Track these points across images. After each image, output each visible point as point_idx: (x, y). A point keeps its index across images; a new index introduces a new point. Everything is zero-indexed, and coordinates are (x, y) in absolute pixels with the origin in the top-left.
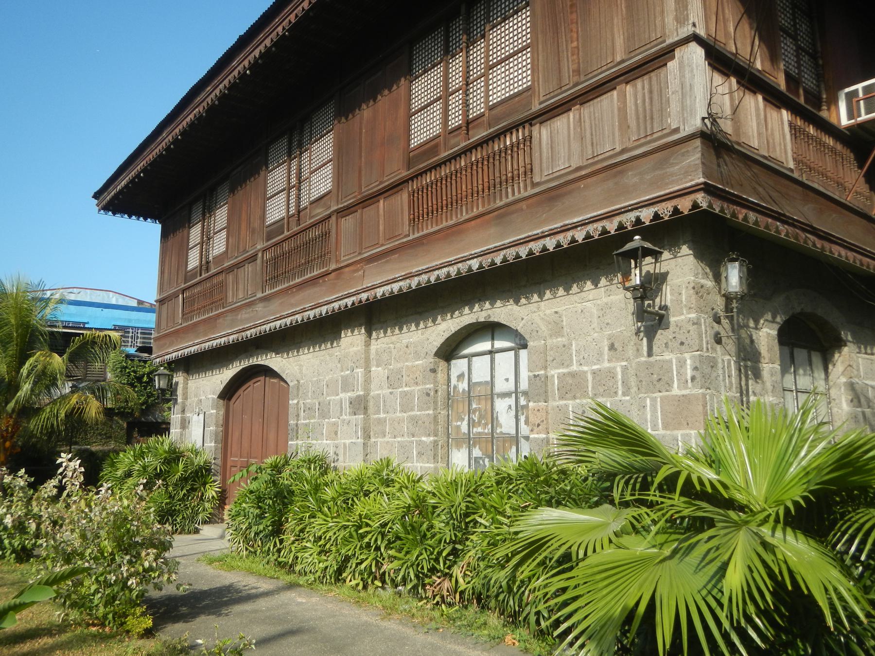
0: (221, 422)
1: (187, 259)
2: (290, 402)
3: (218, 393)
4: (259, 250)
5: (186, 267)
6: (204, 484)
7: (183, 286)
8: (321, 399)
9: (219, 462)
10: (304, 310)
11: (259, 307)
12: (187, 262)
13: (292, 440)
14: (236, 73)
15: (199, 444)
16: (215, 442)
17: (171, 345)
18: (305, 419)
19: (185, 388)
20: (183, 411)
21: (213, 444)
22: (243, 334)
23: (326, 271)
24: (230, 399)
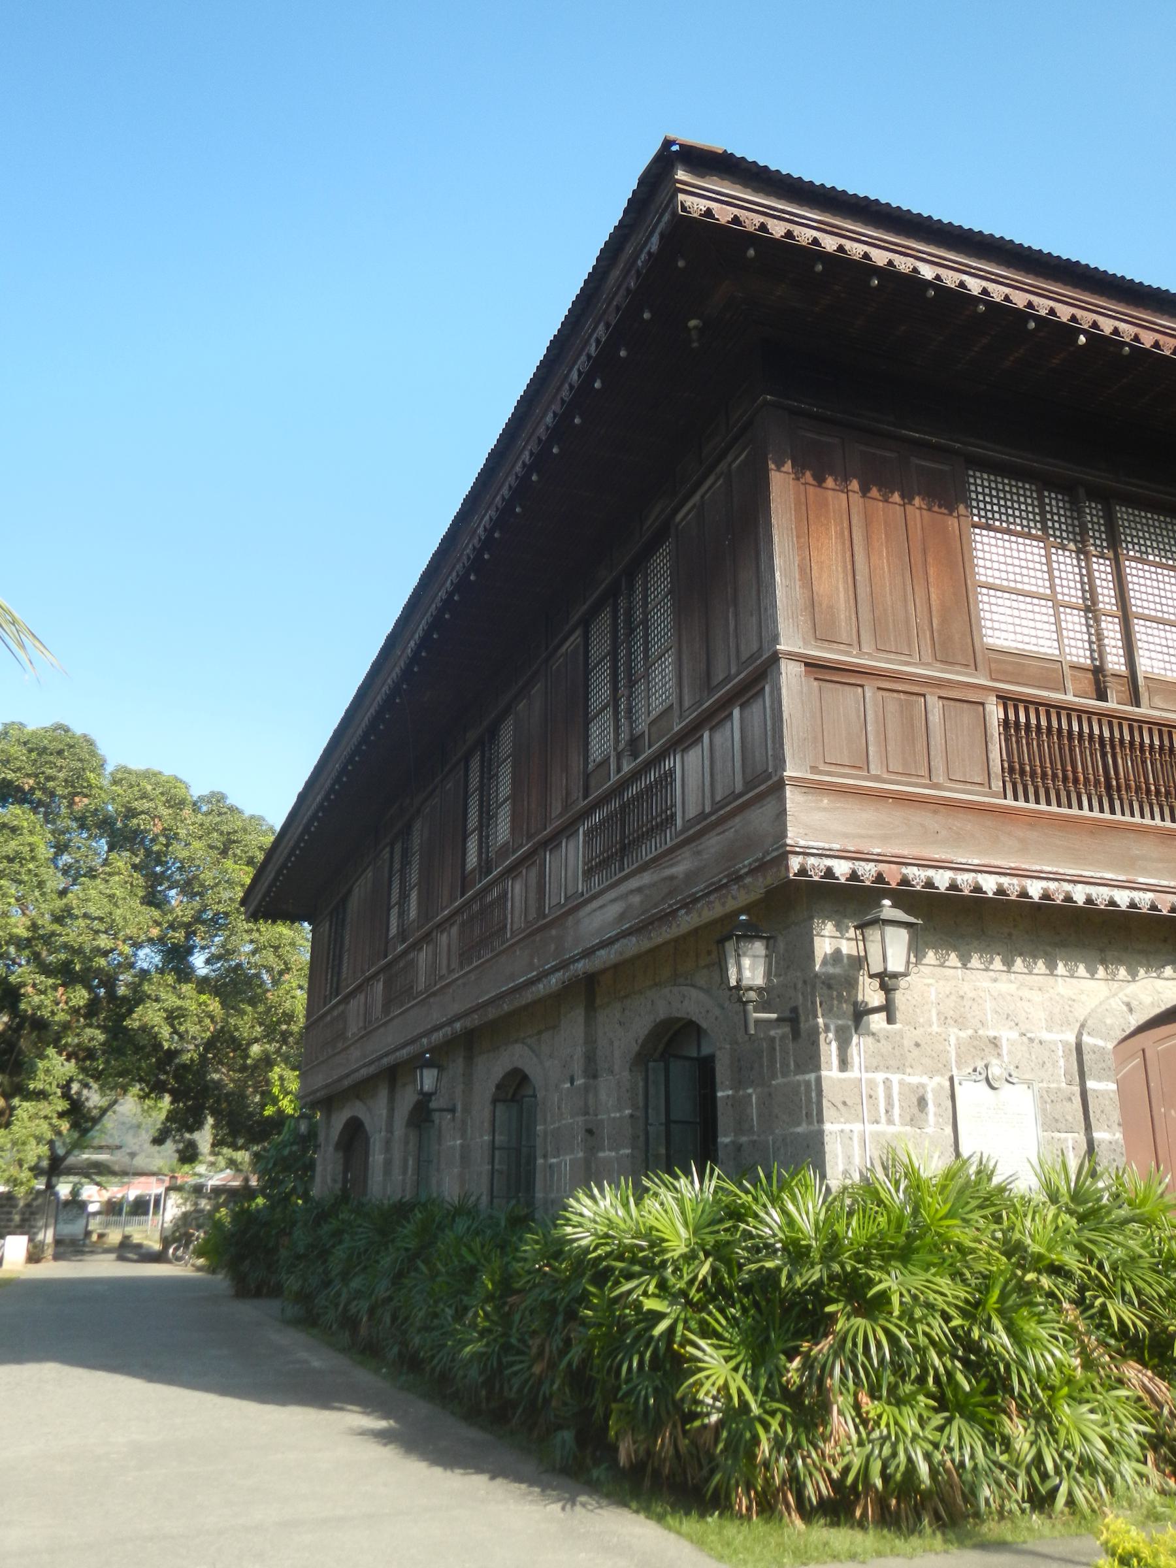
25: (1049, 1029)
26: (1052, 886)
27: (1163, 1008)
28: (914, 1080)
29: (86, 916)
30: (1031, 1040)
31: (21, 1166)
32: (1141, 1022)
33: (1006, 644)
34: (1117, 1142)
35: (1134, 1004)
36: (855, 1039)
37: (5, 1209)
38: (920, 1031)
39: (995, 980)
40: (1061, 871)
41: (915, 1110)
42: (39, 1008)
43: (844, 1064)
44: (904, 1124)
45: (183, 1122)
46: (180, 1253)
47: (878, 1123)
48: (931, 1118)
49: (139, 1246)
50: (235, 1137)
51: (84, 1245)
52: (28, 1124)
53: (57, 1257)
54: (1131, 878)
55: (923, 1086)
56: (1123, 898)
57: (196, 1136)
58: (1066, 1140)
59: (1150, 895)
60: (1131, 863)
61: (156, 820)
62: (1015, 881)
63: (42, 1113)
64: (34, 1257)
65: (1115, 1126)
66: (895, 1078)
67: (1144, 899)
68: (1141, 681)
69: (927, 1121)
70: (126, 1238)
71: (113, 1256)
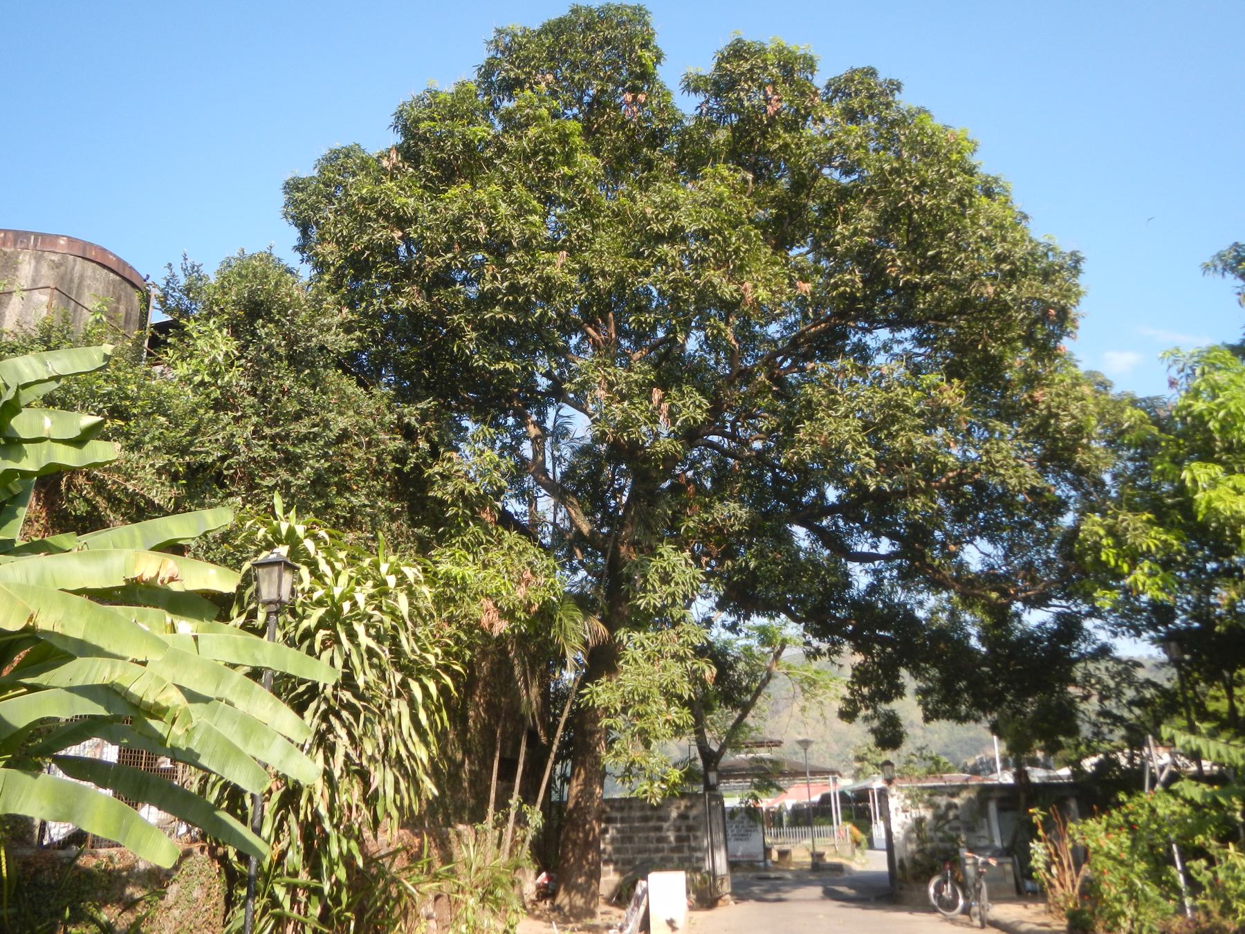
29: (676, 235)
31: (647, 745)
37: (651, 824)
42: (623, 426)
45: (875, 685)
46: (947, 891)
49: (838, 868)
50: (955, 703)
51: (766, 868)
52: (647, 667)
53: (741, 894)
57: (896, 705)
61: (769, 90)
63: (669, 649)
64: (705, 898)
70: (818, 857)
71: (817, 891)
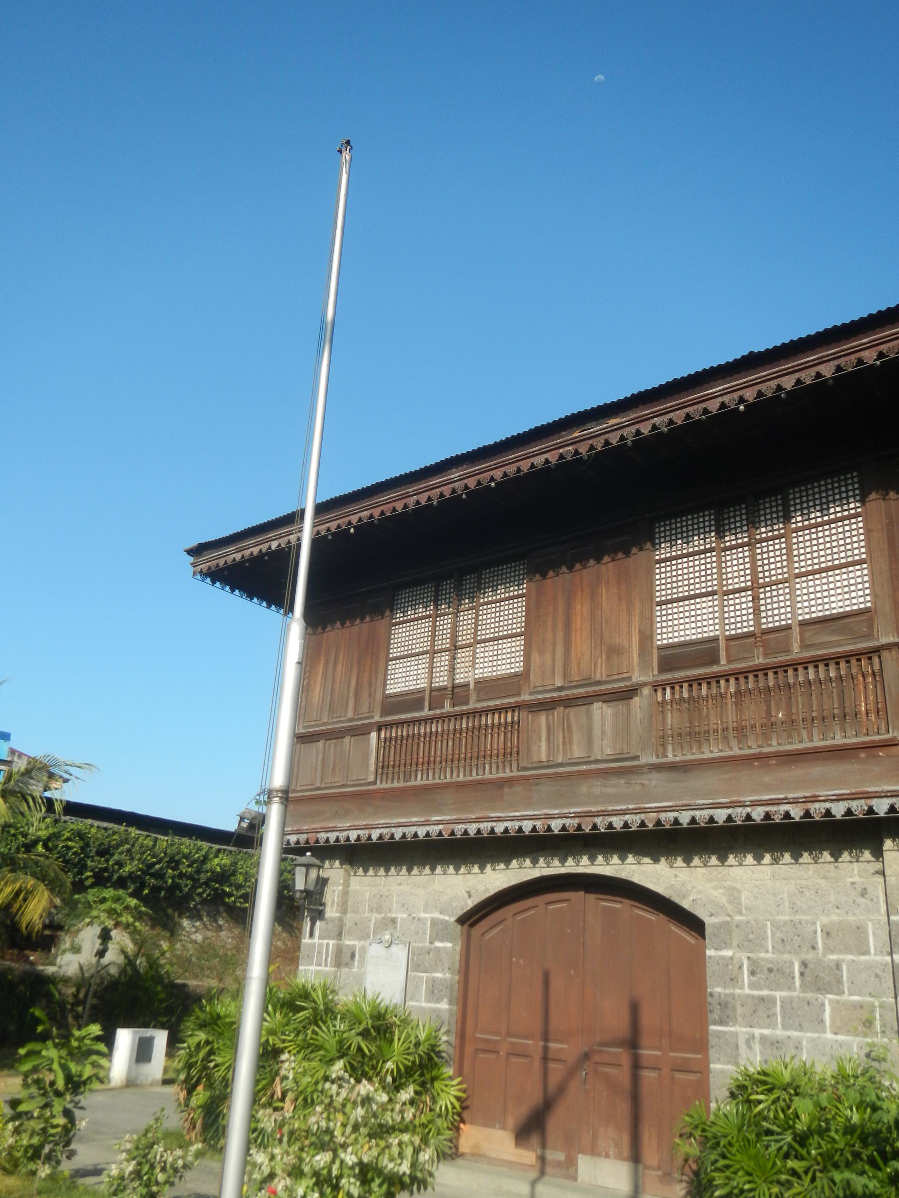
0: (457, 965)
1: (386, 675)
2: (710, 952)
3: (460, 912)
4: (645, 684)
5: (385, 689)
6: (433, 1079)
7: (377, 719)
8: (810, 956)
9: (452, 1039)
10: (815, 799)
11: (654, 780)
12: (385, 680)
13: (721, 1023)
14: (713, 406)
15: (398, 999)
16: (450, 1003)
17: (336, 816)
18: (752, 986)
19: (345, 893)
20: (340, 935)
21: (444, 1006)
22: (598, 820)
23: (886, 740)
24: (472, 925)
25: (425, 911)
26: (385, 831)
27: (492, 892)
28: (352, 943)
30: (414, 918)
32: (475, 903)
33: (395, 691)
34: (445, 979)
35: (473, 892)
36: (318, 923)
38: (359, 916)
39: (400, 884)
40: (388, 821)
41: (348, 959)
43: (311, 935)
44: (331, 966)
47: (320, 965)
48: (356, 963)
54: (427, 818)
55: (355, 946)
56: (422, 832)
58: (423, 977)
59: (441, 827)
60: (437, 810)
62: (367, 832)
65: (447, 969)
66: (331, 942)
67: (434, 830)
68: (472, 686)
69: (354, 965)
